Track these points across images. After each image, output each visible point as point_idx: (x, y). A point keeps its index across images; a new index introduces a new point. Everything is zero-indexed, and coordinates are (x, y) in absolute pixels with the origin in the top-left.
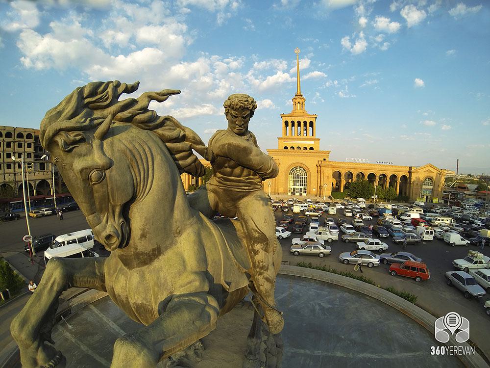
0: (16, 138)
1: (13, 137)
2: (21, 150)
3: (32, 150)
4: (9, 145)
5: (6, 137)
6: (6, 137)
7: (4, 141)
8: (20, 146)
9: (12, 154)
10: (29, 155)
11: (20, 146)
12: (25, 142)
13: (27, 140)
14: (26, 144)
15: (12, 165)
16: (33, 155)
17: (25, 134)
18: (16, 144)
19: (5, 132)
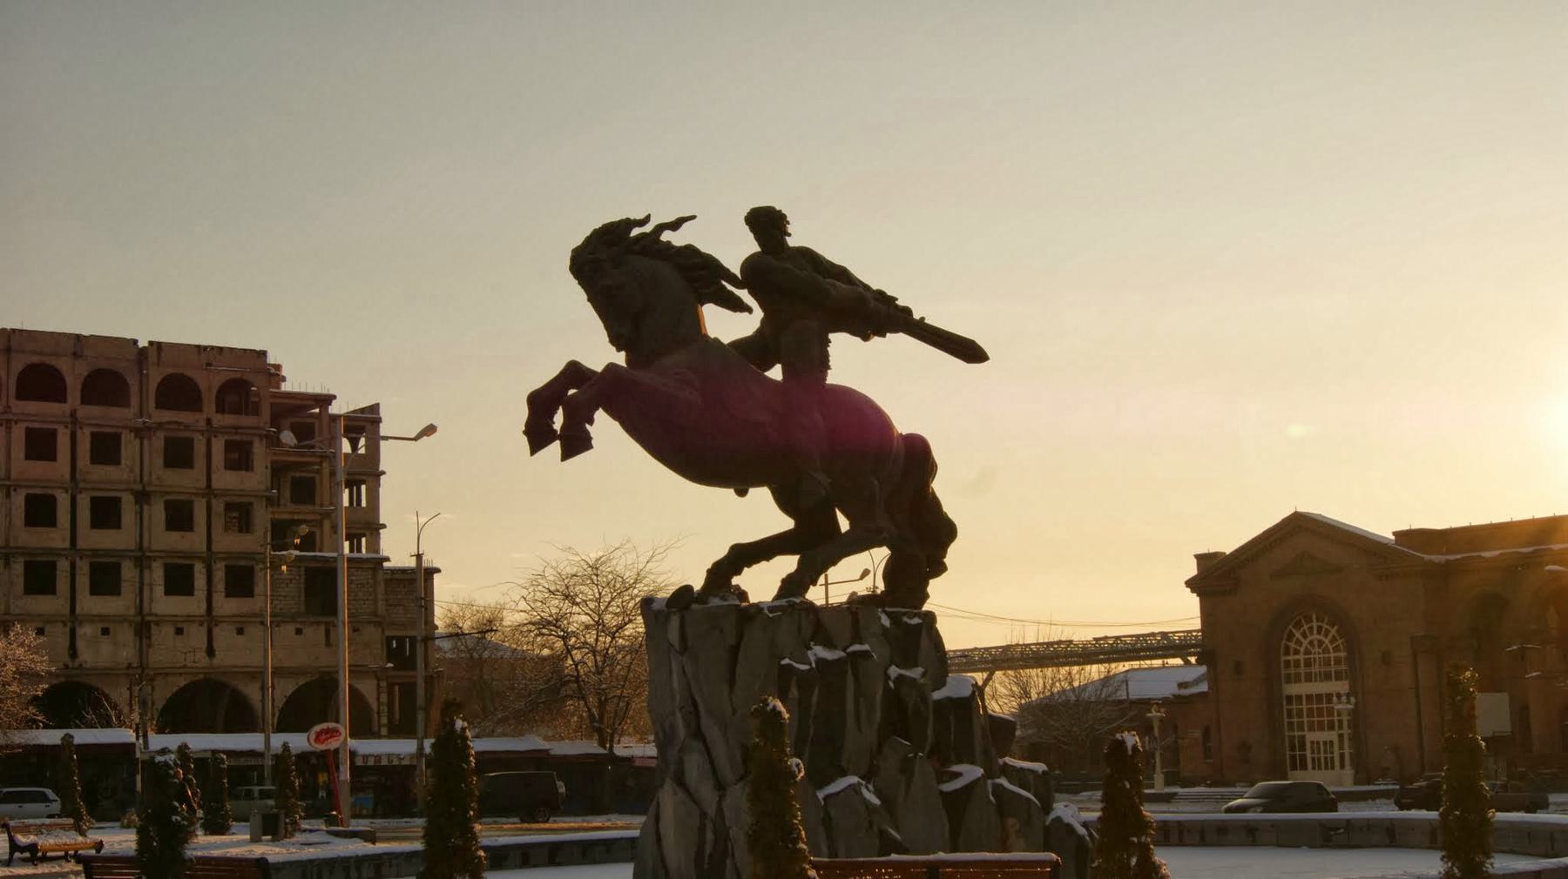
0: (152, 404)
1: (134, 401)
2: (184, 481)
3: (256, 480)
4: (106, 449)
5: (86, 399)
6: (86, 399)
7: (74, 421)
8: (178, 454)
9: (127, 501)
10: (240, 514)
11: (178, 454)
12: (210, 430)
13: (220, 420)
14: (218, 446)
15: (128, 571)
16: (262, 517)
17: (208, 384)
18: (159, 441)
19: (83, 369)
